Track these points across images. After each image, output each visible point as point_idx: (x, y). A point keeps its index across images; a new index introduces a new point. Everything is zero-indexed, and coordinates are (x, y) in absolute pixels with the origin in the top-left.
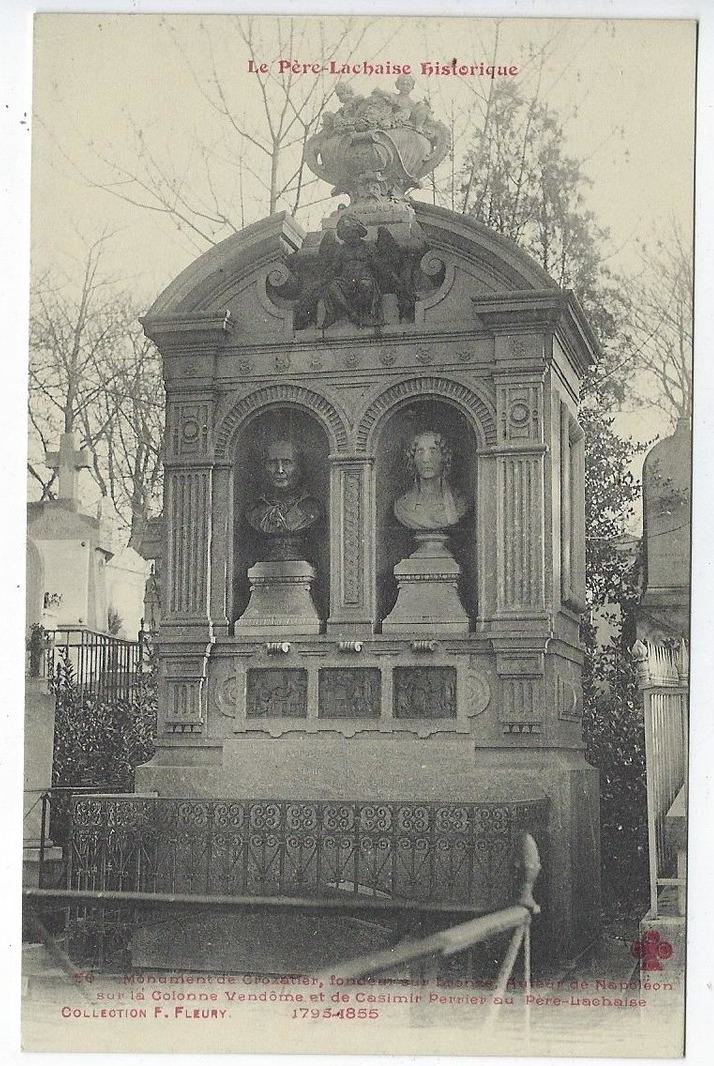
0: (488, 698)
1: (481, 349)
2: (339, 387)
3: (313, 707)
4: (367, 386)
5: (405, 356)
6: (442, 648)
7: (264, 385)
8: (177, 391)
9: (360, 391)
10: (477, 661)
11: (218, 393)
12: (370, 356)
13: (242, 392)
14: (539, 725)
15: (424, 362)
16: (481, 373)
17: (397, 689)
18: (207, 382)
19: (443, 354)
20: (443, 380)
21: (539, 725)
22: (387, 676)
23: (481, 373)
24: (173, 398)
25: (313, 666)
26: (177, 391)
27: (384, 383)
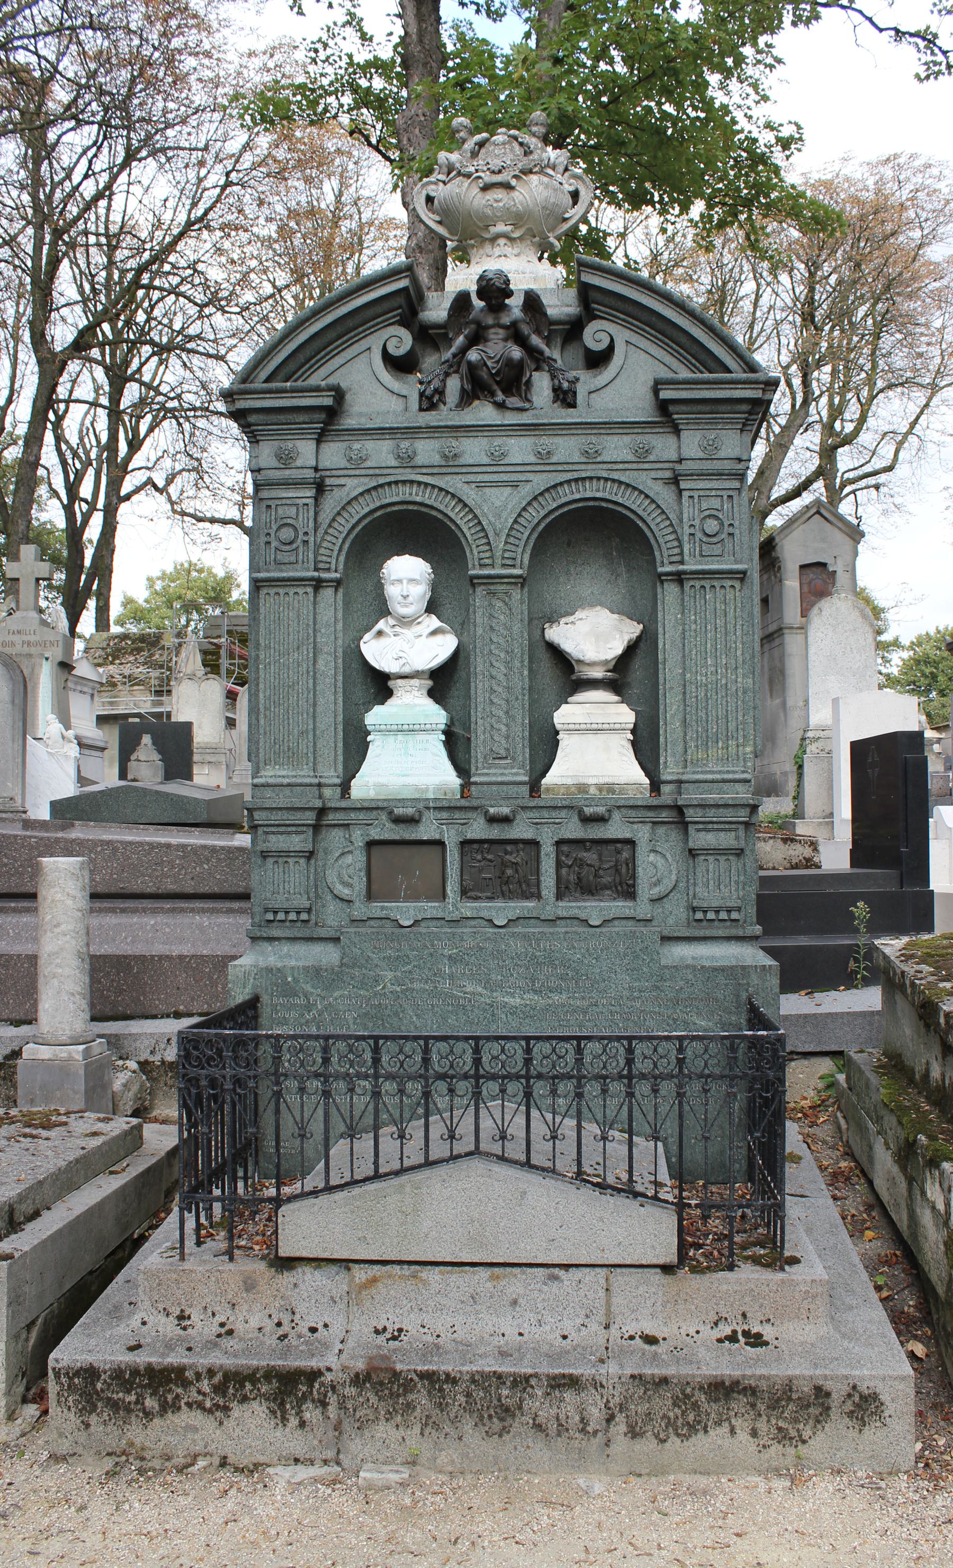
0: (674, 877)
1: (663, 446)
2: (480, 486)
3: (452, 888)
4: (515, 485)
5: (566, 448)
6: (616, 815)
7: (382, 480)
8: (271, 484)
9: (508, 490)
10: (661, 830)
11: (320, 488)
12: (520, 449)
13: (354, 486)
14: (739, 909)
15: (590, 457)
16: (660, 474)
17: (559, 865)
18: (310, 474)
19: (617, 448)
20: (614, 481)
21: (739, 909)
22: (548, 849)
23: (660, 474)
24: (264, 494)
25: (451, 838)
26: (271, 484)
27: (540, 481)
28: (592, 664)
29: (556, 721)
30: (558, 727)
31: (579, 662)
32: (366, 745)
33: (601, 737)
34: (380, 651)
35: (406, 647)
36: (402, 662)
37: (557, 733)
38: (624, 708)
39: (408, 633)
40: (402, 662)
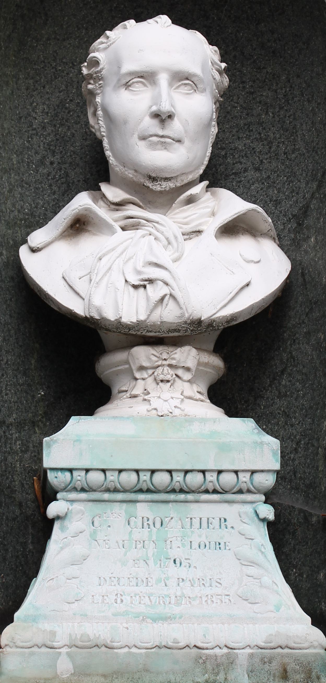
32: (46, 527)
34: (83, 267)
35: (165, 257)
36: (155, 292)
39: (171, 222)
40: (155, 292)
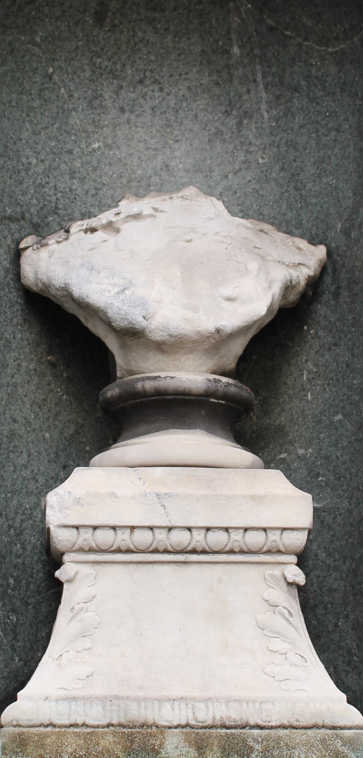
28: (172, 346)
29: (53, 518)
30: (61, 538)
31: (132, 335)
33: (199, 578)
37: (54, 560)
38: (275, 482)
